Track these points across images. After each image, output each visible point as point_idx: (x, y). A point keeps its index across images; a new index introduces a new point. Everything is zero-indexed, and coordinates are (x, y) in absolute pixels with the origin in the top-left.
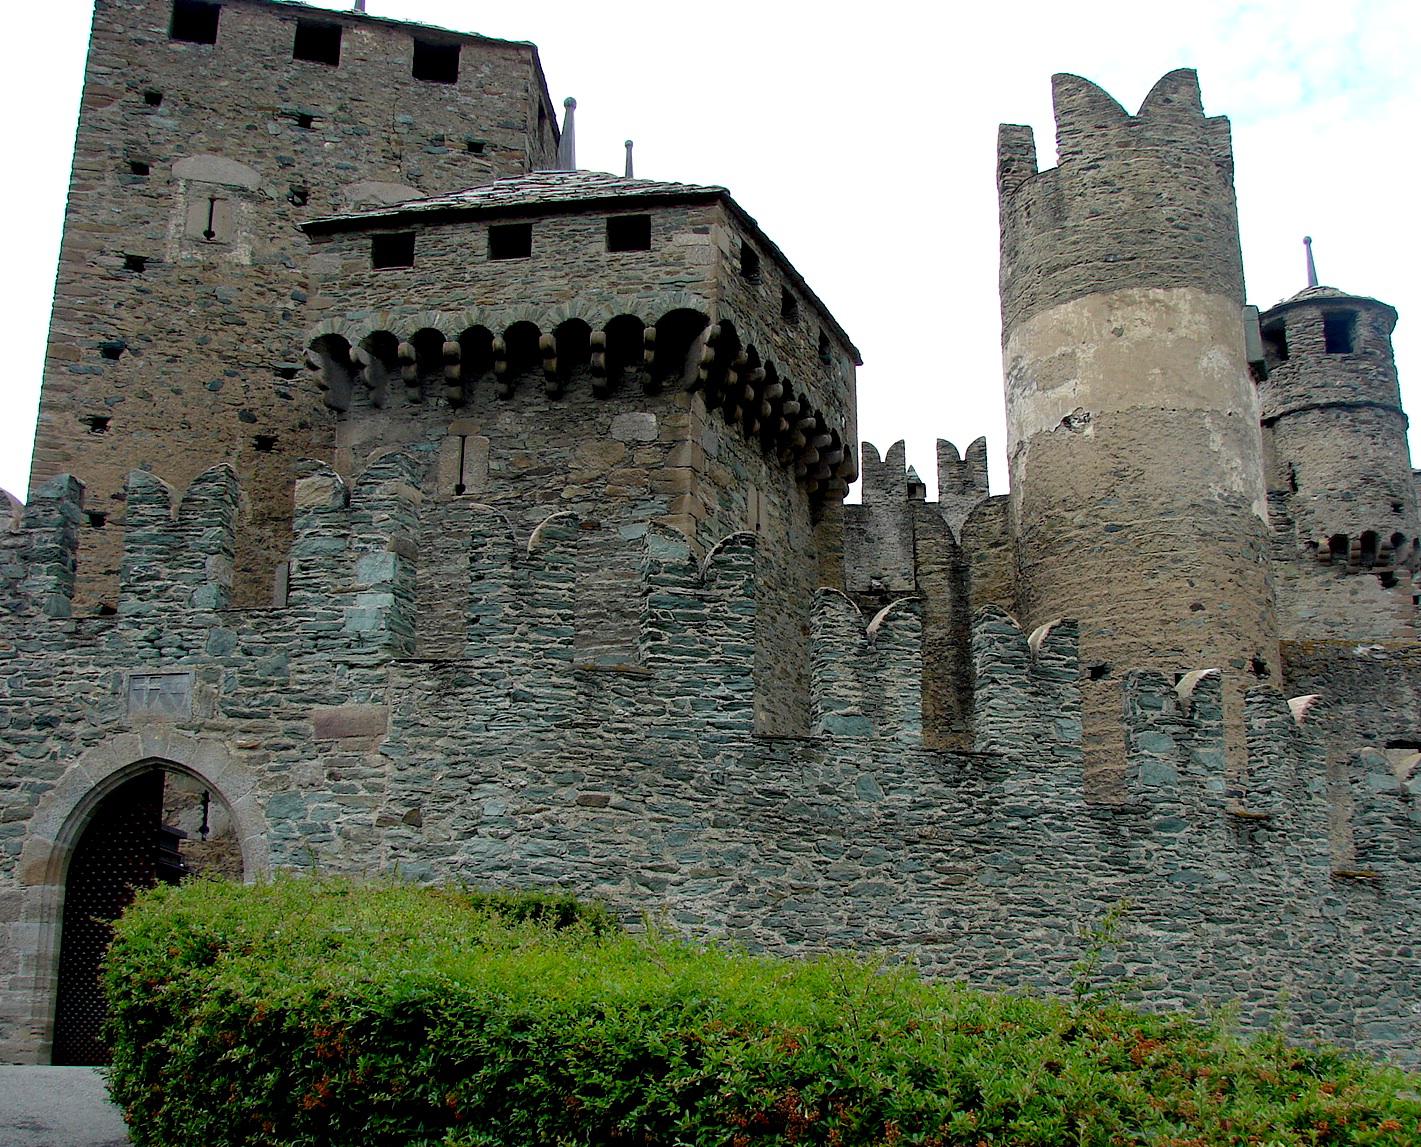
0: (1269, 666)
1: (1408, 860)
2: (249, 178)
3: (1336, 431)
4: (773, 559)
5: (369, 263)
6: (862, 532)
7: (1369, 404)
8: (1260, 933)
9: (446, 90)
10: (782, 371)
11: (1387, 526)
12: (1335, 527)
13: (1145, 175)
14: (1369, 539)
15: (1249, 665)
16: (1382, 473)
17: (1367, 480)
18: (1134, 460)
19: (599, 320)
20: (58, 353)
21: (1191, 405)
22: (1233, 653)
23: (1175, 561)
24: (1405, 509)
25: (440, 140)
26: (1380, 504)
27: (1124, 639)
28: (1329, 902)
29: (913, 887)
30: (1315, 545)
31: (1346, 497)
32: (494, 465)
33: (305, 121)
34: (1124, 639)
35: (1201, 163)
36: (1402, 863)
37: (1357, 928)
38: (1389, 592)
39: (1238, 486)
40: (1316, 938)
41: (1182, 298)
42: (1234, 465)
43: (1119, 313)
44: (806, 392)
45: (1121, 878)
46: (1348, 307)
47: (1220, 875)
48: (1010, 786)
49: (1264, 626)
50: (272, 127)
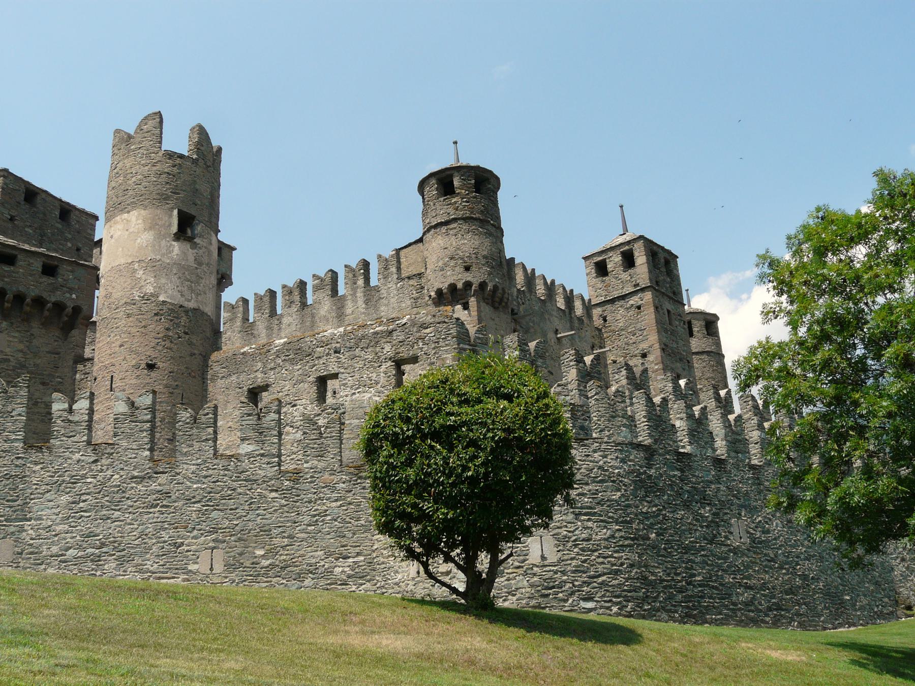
0: (160, 364)
1: (68, 437)
3: (439, 237)
4: (9, 357)
6: (252, 334)
7: (455, 220)
12: (437, 285)
13: (128, 165)
14: (453, 287)
15: (143, 366)
16: (460, 252)
18: (110, 290)
21: (130, 261)
22: (134, 362)
23: (116, 328)
24: (473, 268)
26: (457, 269)
27: (101, 364)
28: (18, 458)
30: (430, 296)
31: (442, 270)
34: (101, 364)
35: (154, 153)
36: (65, 439)
37: (38, 467)
38: (466, 312)
39: (150, 289)
40: (6, 472)
41: (134, 213)
42: (148, 281)
43: (112, 228)
44: (22, 289)
46: (449, 173)
49: (160, 348)
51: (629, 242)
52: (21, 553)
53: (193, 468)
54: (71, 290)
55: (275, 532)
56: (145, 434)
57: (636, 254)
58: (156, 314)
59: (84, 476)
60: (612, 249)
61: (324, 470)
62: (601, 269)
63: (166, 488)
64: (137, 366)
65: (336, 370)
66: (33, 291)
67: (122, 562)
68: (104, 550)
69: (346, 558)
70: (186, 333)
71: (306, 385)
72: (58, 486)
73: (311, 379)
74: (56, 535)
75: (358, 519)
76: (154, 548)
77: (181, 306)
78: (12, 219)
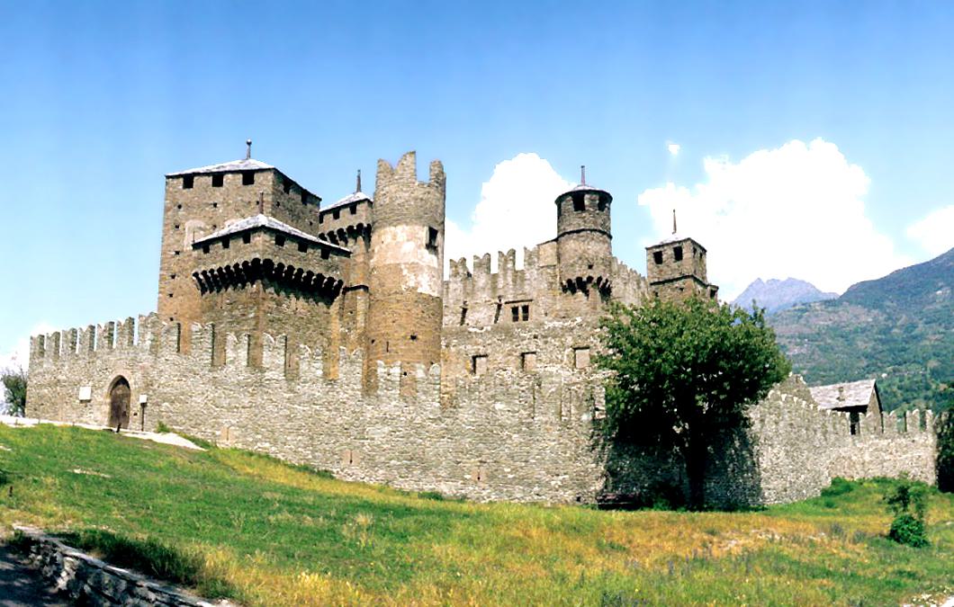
0: (420, 337)
2: (202, 225)
5: (202, 253)
7: (583, 230)
8: (330, 408)
9: (250, 187)
10: (297, 267)
11: (584, 274)
14: (579, 279)
17: (580, 258)
19: (241, 262)
20: (162, 278)
22: (403, 334)
24: (594, 267)
25: (250, 202)
29: (243, 396)
30: (562, 283)
31: (572, 265)
32: (228, 301)
33: (215, 205)
37: (370, 408)
39: (412, 284)
44: (311, 269)
45: (292, 395)
47: (318, 394)
48: (266, 374)
50: (207, 209)
51: (679, 242)
52: (363, 459)
53: (466, 416)
54: (337, 269)
55: (516, 458)
56: (436, 392)
57: (684, 251)
58: (416, 302)
59: (399, 416)
60: (667, 244)
61: (546, 423)
62: (658, 258)
63: (450, 427)
64: (405, 337)
65: (534, 350)
66: (317, 270)
67: (425, 470)
68: (413, 462)
69: (558, 475)
70: (433, 315)
71: (513, 358)
72: (384, 421)
73: (518, 354)
74: (384, 451)
75: (566, 453)
76: (444, 463)
77: (430, 296)
78: (278, 204)
